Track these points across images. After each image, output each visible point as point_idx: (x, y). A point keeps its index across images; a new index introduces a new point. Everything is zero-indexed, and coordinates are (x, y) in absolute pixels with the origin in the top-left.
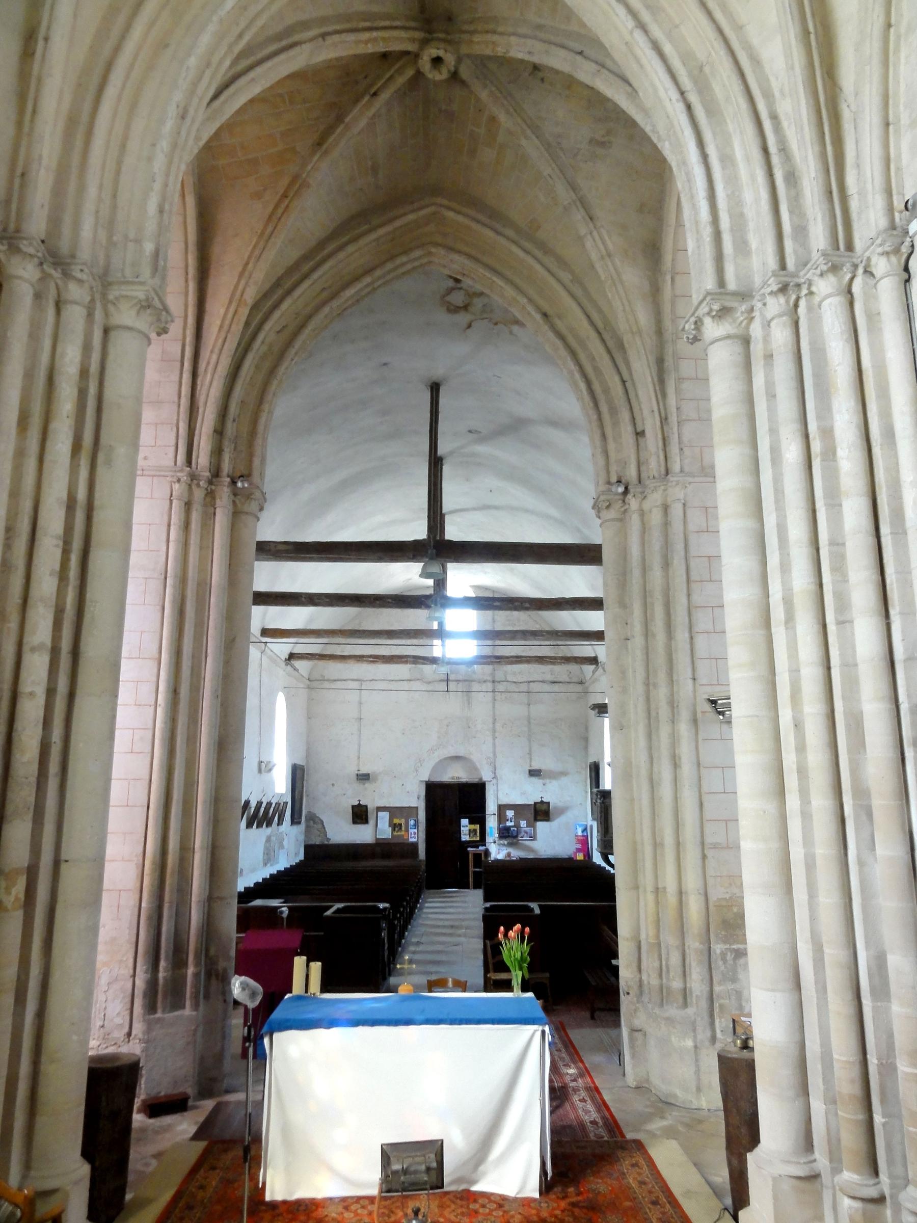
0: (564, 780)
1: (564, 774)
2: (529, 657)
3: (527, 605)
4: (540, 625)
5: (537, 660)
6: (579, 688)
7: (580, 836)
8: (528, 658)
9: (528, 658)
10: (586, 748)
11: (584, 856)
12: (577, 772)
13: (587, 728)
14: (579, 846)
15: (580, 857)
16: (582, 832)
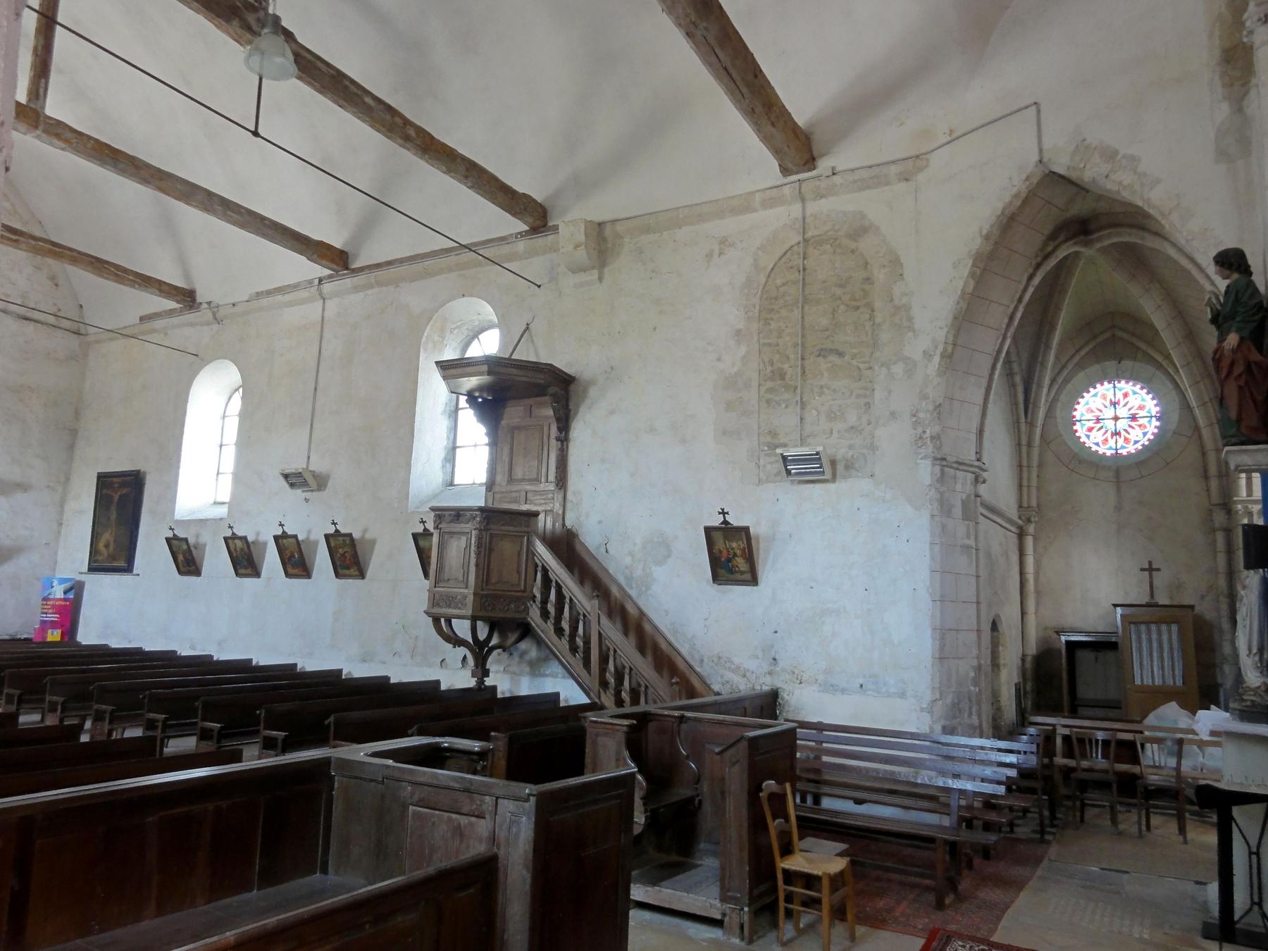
0: (20, 497)
1: (23, 487)
2: (79, 252)
3: (412, 133)
4: (12, 205)
5: (92, 263)
6: (74, 341)
7: (60, 600)
8: (75, 254)
9: (75, 254)
10: (71, 447)
11: (63, 635)
12: (48, 487)
13: (77, 413)
14: (53, 617)
15: (54, 636)
16: (65, 593)
